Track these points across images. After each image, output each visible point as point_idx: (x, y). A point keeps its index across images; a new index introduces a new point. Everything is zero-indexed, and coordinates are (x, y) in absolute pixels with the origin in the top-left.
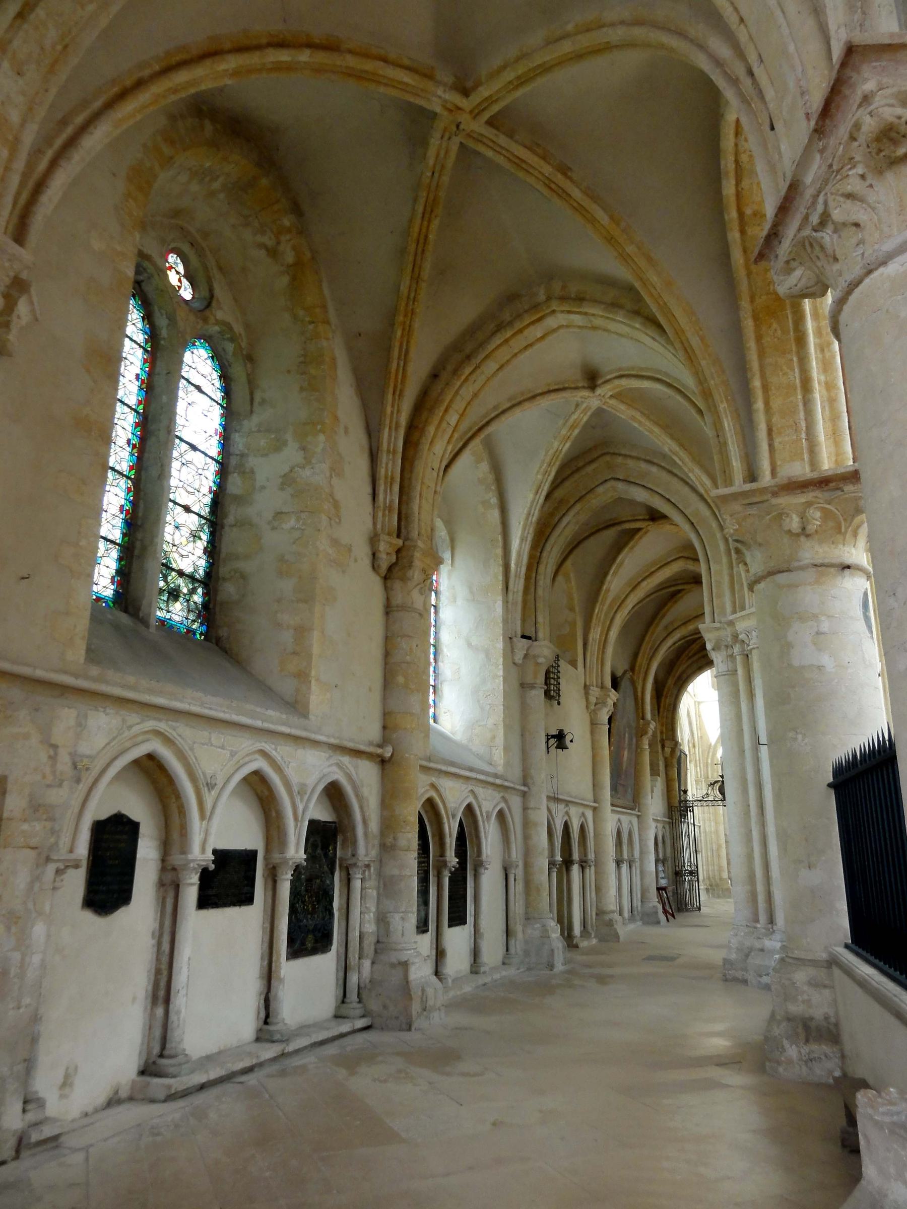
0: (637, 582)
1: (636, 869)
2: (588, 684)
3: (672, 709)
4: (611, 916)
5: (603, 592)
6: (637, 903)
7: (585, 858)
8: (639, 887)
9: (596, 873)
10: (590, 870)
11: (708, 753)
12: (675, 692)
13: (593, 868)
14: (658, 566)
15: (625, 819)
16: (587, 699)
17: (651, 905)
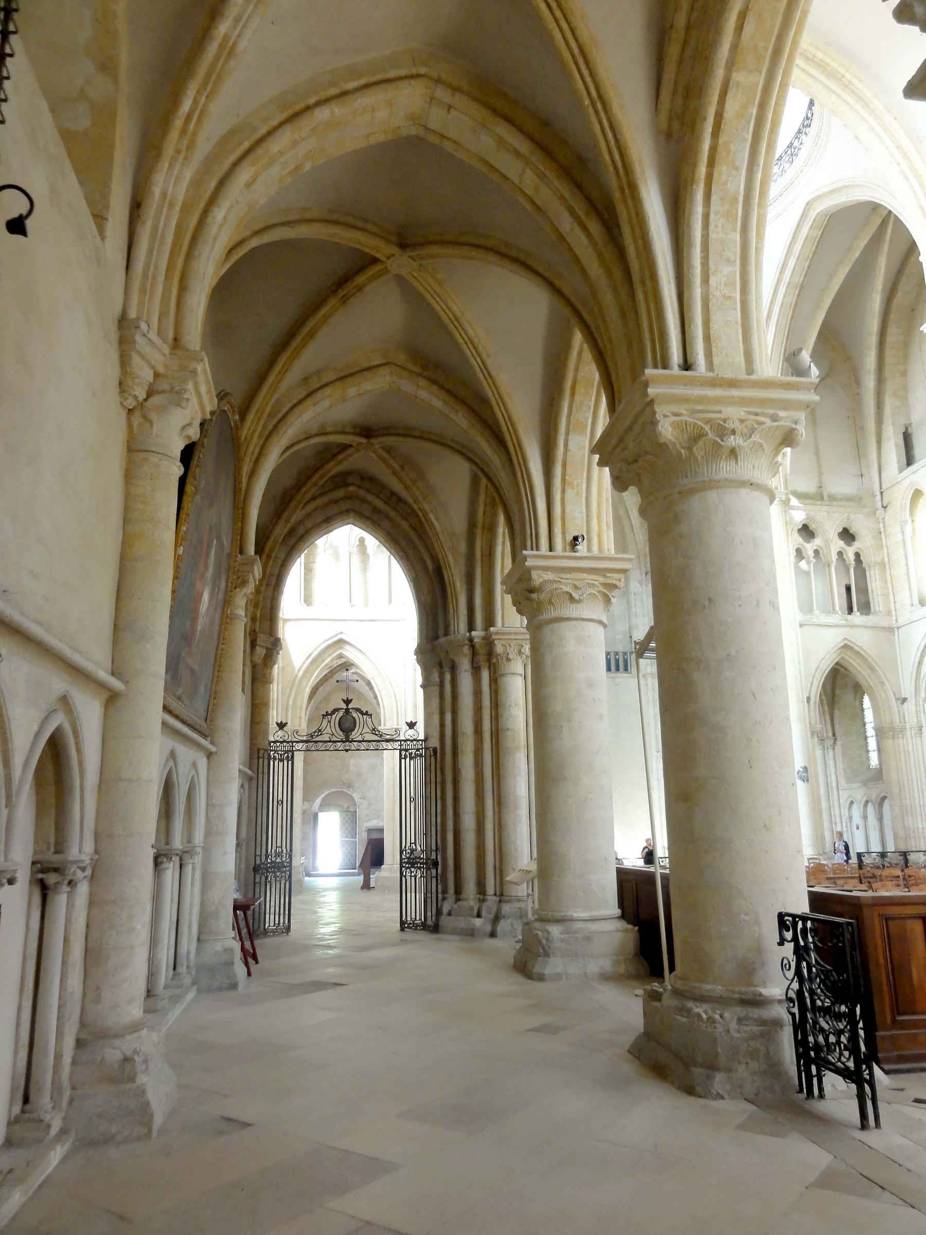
0: (302, 105)
1: (194, 869)
2: (132, 314)
3: (273, 584)
4: (127, 1045)
5: (212, 49)
6: (188, 945)
7: (57, 858)
8: (196, 910)
9: (91, 904)
10: (71, 895)
11: (291, 690)
12: (282, 556)
13: (83, 889)
14: (363, 81)
15: (186, 754)
16: (124, 361)
17: (219, 947)
